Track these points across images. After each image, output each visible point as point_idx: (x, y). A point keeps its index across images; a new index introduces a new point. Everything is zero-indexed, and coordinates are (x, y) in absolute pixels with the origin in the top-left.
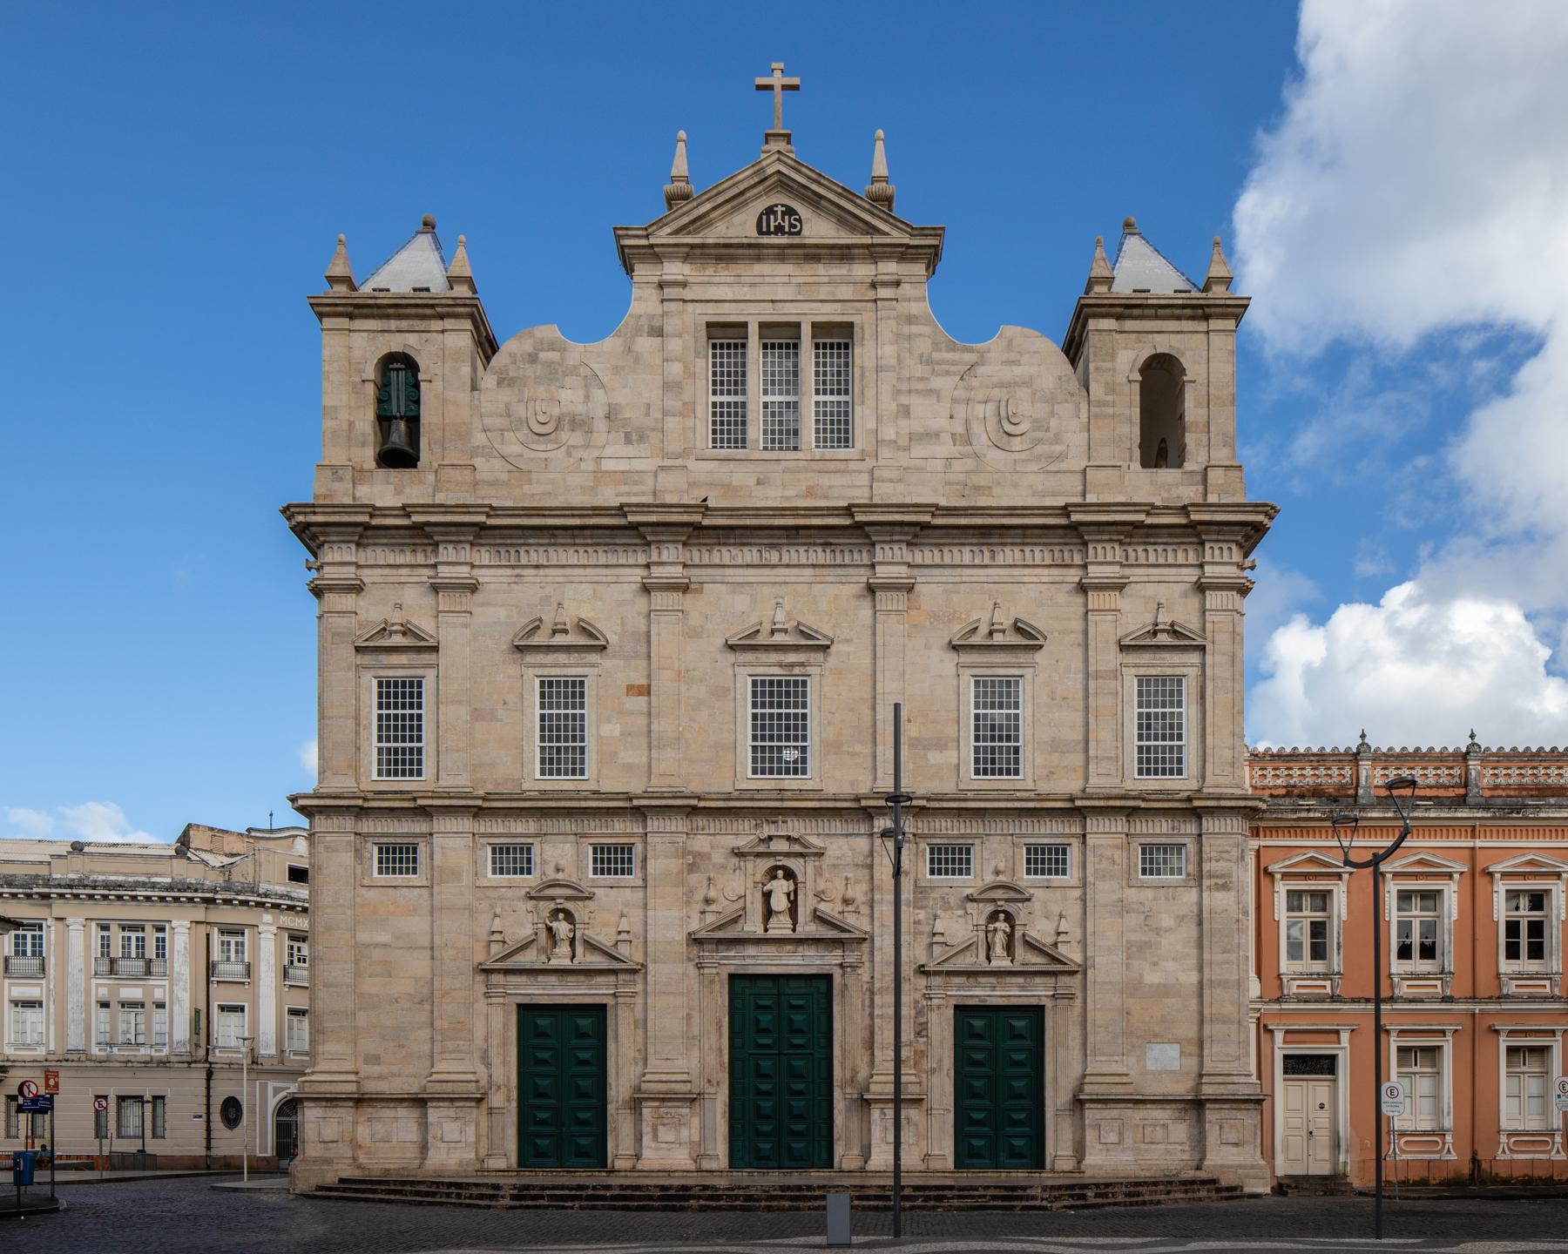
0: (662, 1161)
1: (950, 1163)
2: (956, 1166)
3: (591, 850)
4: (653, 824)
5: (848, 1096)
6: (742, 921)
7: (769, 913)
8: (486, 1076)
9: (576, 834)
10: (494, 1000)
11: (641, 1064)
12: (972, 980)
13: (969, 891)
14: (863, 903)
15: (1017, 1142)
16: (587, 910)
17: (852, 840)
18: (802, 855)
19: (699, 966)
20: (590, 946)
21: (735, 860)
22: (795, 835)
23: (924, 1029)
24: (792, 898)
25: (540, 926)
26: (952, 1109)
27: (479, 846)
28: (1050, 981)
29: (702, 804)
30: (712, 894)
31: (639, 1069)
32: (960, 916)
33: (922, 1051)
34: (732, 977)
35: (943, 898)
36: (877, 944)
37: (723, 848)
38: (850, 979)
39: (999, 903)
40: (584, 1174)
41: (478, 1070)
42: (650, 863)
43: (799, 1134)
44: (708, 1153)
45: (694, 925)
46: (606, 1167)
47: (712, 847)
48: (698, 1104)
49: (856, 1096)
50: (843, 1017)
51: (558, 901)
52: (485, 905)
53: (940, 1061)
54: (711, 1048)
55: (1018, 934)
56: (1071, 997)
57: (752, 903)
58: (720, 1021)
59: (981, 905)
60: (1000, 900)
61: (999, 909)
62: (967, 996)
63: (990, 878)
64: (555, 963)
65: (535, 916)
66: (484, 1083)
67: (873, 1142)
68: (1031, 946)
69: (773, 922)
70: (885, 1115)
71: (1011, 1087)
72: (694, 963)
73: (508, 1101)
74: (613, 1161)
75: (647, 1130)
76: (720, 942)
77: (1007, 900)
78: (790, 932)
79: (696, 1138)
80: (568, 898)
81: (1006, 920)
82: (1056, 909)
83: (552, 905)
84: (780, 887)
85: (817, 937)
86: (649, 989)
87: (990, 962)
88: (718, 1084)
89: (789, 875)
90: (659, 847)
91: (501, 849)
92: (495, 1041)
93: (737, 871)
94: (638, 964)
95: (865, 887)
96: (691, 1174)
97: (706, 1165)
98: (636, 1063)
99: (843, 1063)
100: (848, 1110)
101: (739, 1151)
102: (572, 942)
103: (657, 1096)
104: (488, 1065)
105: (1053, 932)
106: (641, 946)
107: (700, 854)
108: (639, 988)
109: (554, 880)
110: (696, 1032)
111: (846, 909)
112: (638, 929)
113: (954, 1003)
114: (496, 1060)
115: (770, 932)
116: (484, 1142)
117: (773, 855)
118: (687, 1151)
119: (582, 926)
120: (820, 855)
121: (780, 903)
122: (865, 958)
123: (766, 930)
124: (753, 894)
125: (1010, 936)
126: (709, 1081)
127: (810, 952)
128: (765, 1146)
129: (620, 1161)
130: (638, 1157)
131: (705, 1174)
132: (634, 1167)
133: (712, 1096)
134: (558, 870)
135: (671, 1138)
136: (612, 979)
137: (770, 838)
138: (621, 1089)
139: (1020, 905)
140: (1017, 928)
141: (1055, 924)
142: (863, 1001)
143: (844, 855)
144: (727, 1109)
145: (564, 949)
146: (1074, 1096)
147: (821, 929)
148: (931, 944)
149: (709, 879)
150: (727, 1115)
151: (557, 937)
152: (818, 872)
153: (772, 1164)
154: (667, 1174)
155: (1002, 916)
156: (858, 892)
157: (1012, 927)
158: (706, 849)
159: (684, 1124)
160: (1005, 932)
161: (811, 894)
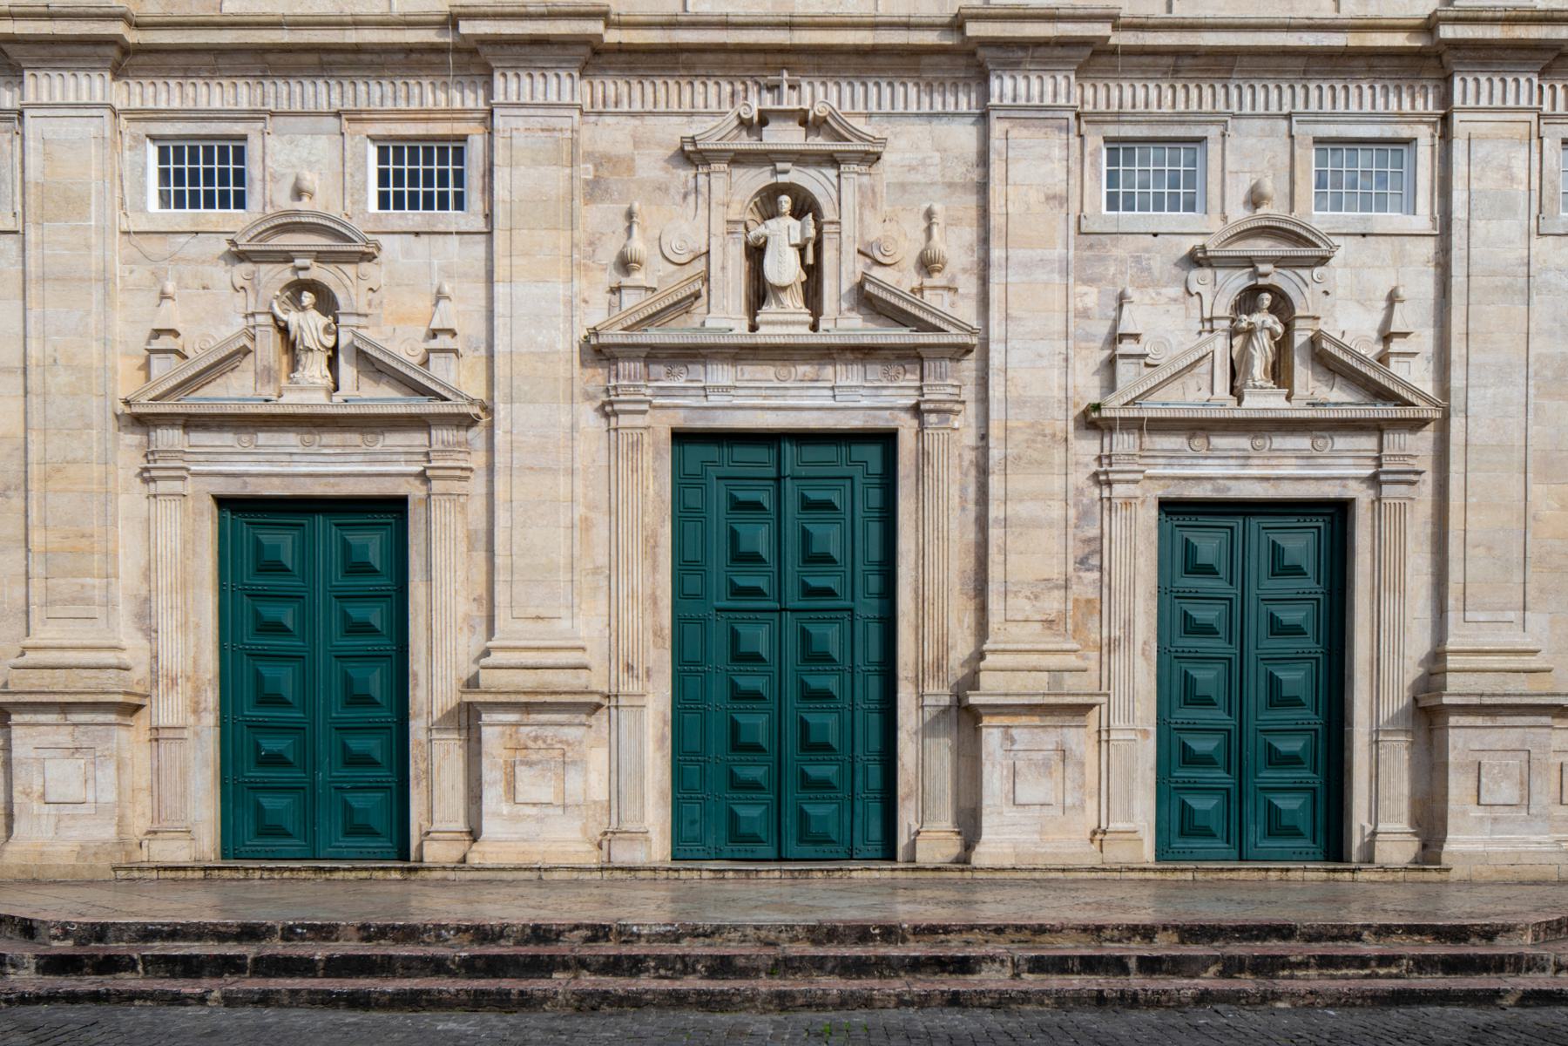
0: (525, 846)
1: (1148, 852)
2: (1158, 859)
3: (373, 152)
4: (507, 86)
5: (928, 701)
6: (700, 307)
7: (759, 293)
8: (145, 657)
9: (338, 114)
10: (162, 486)
11: (482, 629)
12: (1198, 442)
13: (1198, 241)
14: (964, 271)
15: (1286, 803)
16: (365, 285)
17: (940, 127)
18: (832, 160)
19: (607, 411)
20: (372, 365)
21: (685, 174)
22: (820, 110)
23: (1092, 553)
25: (260, 319)
26: (1153, 729)
27: (127, 140)
28: (1368, 443)
29: (613, 37)
30: (638, 246)
31: (478, 642)
32: (1175, 300)
33: (1088, 601)
34: (681, 437)
35: (1138, 260)
36: (996, 359)
37: (660, 145)
38: (933, 440)
39: (1263, 268)
40: (352, 875)
41: (125, 643)
42: (501, 176)
43: (825, 785)
44: (625, 827)
45: (596, 314)
46: (406, 858)
47: (637, 144)
48: (602, 716)
49: (946, 701)
50: (920, 526)
51: (299, 262)
52: (142, 273)
53: (1129, 624)
54: (632, 595)
55: (1300, 339)
56: (1409, 478)
57: (723, 268)
58: (655, 535)
59: (1221, 274)
60: (1265, 260)
61: (1261, 281)
62: (1186, 479)
63: (1239, 214)
64: (294, 400)
65: (251, 298)
66: (140, 672)
67: (987, 801)
68: (1328, 363)
69: (768, 312)
70: (1013, 741)
71: (1274, 683)
72: (598, 403)
73: (196, 712)
74: (421, 846)
75: (491, 774)
76: (654, 354)
77: (1280, 262)
78: (806, 330)
79: (599, 791)
80: (322, 257)
81: (1272, 310)
83: (285, 274)
84: (785, 233)
85: (867, 341)
86: (500, 460)
87: (1240, 400)
88: (648, 672)
89: (804, 206)
90: (519, 140)
91: (179, 151)
92: (164, 579)
93: (692, 198)
94: (472, 402)
95: (969, 234)
96: (586, 876)
97: (623, 854)
98: (472, 628)
99: (919, 629)
100: (927, 730)
101: (693, 822)
103: (513, 698)
104: (150, 632)
105: (1375, 335)
106: (481, 367)
107: (609, 159)
108: (478, 460)
109: (287, 214)
110: (602, 560)
111: (928, 282)
112: (471, 327)
113: (1161, 493)
114: (167, 623)
115: (763, 330)
116: (144, 801)
118: (578, 824)
119: (354, 320)
120: (871, 158)
121: (783, 267)
122: (969, 393)
123: (753, 328)
124: (724, 247)
125: (1283, 346)
126: (629, 668)
127: (849, 375)
128: (752, 813)
129: (436, 845)
130: (474, 834)
131: (618, 874)
132: (464, 860)
133: (636, 702)
134: (298, 193)
135: (545, 793)
136: (418, 439)
138: (437, 685)
139: (1305, 273)
140: (1298, 324)
141: (1379, 317)
142: (963, 489)
143: (923, 163)
144: (668, 731)
145: (315, 369)
146: (1415, 700)
147: (870, 325)
148: (1111, 362)
149: (630, 215)
150: (668, 743)
151: (299, 347)
152: (869, 198)
153: (767, 850)
154: (533, 875)
155: (1266, 299)
156: (955, 246)
157: (1289, 327)
158: (624, 148)
159: (574, 763)
160: (1272, 337)
161: (850, 250)
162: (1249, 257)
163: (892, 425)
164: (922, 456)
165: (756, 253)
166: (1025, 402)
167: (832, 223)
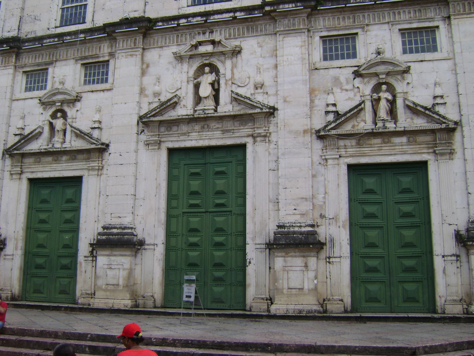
7: (198, 100)
24: (216, 87)
25: (46, 122)
39: (381, 77)
60: (382, 74)
77: (388, 74)
78: (212, 111)
81: (387, 91)
82: (431, 79)
89: (214, 69)
102: (65, 131)
117: (203, 55)
137: (200, 43)
140: (398, 95)
155: (384, 87)
157: (394, 96)
160: (388, 100)
162: (376, 73)
163: (243, 142)
164: (255, 152)
165: (197, 87)
166: (292, 131)
167: (223, 74)
